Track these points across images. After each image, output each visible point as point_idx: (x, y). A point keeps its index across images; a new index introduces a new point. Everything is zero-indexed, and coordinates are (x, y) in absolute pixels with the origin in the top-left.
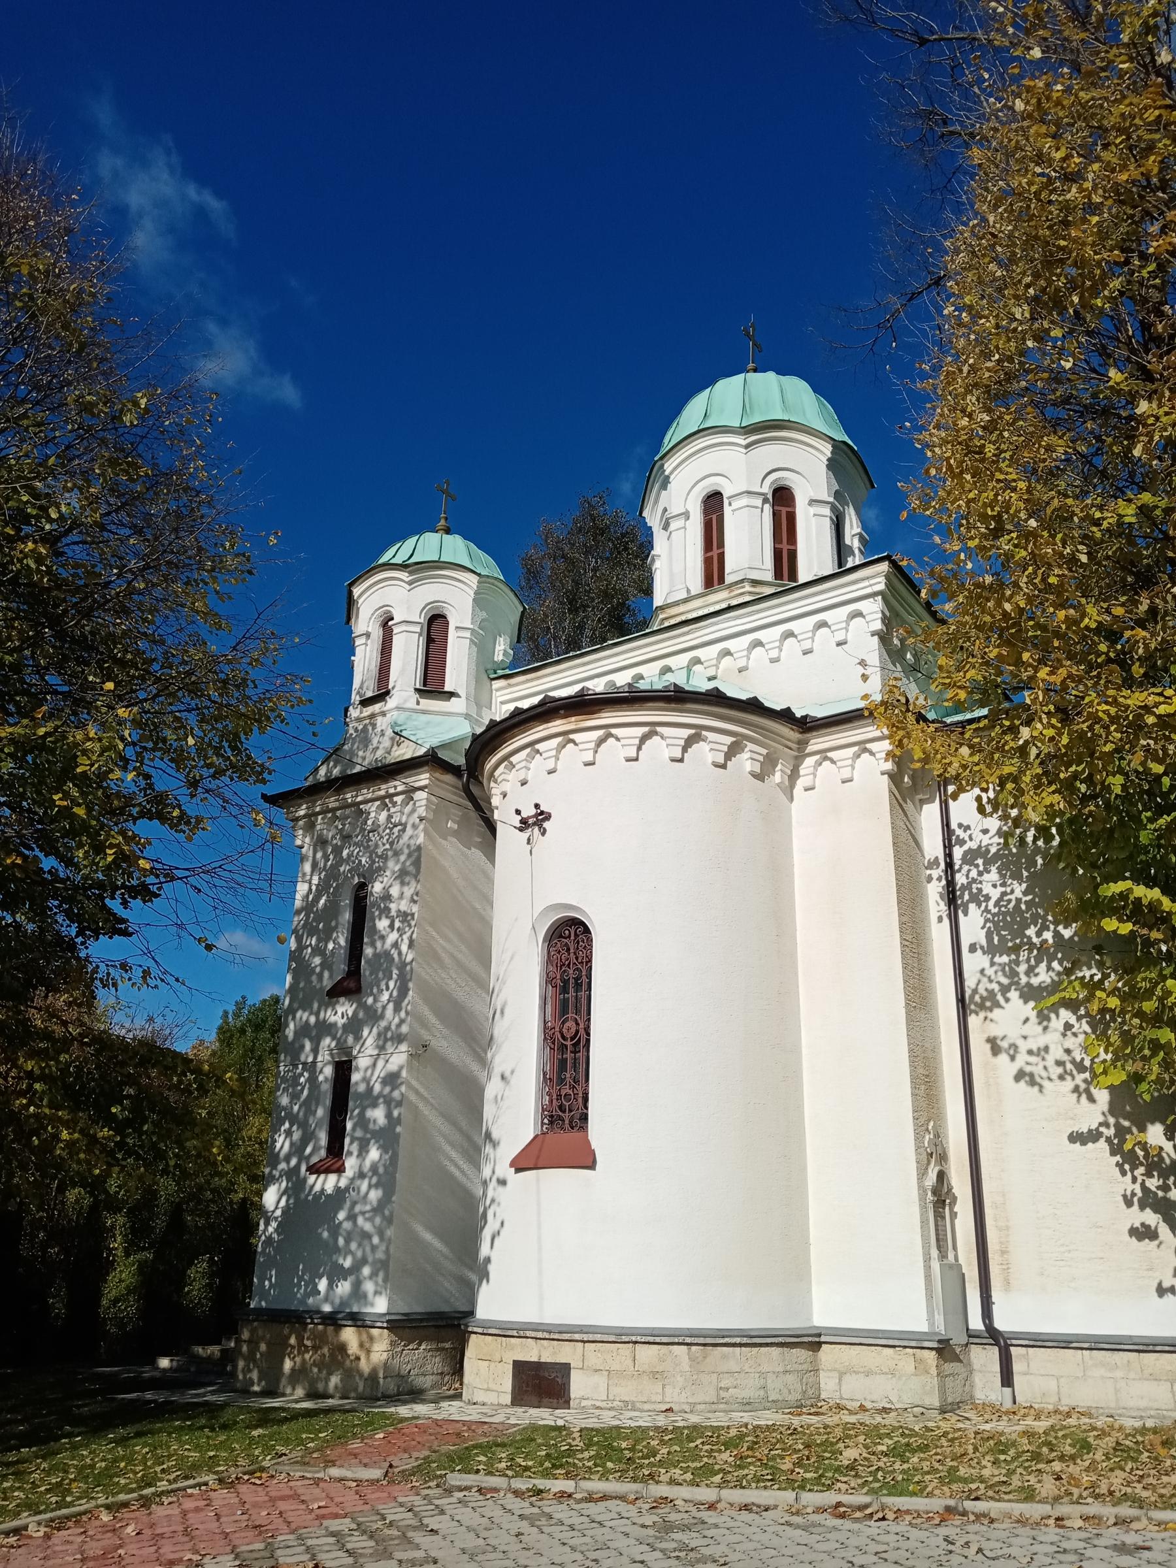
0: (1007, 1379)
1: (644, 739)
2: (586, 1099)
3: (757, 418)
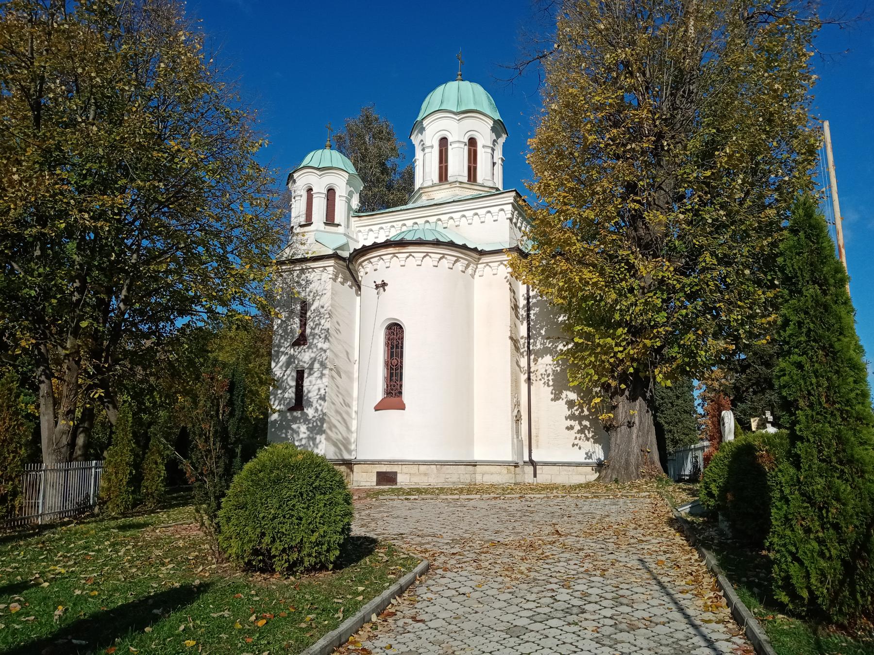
0: (535, 476)
1: (425, 257)
2: (401, 386)
3: (464, 109)
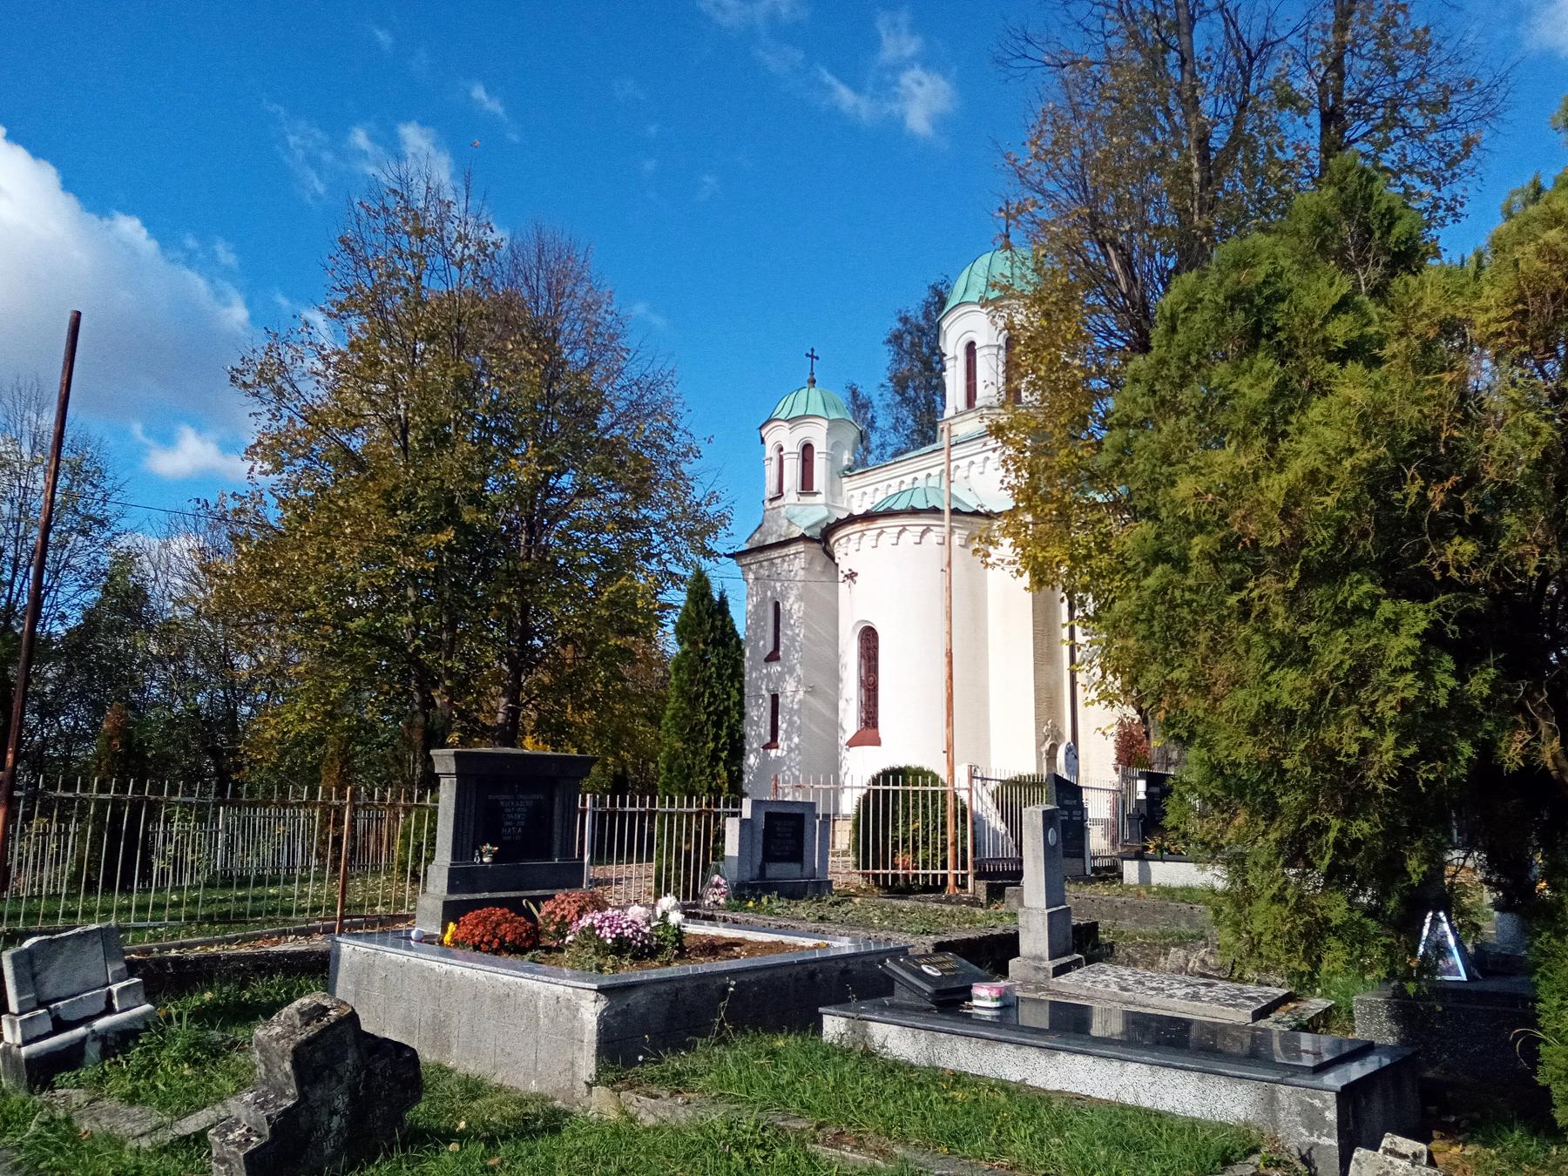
1: (900, 533)
